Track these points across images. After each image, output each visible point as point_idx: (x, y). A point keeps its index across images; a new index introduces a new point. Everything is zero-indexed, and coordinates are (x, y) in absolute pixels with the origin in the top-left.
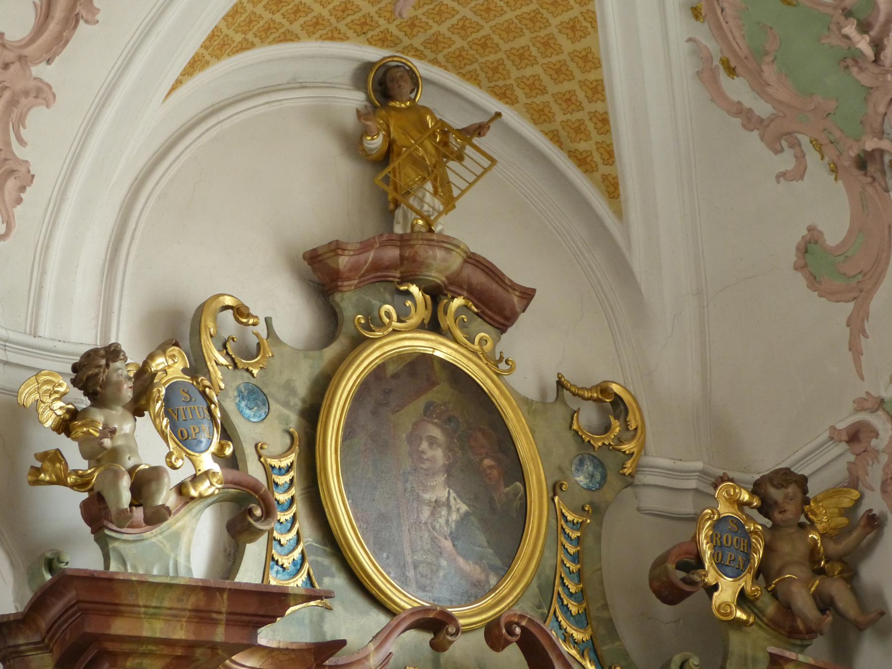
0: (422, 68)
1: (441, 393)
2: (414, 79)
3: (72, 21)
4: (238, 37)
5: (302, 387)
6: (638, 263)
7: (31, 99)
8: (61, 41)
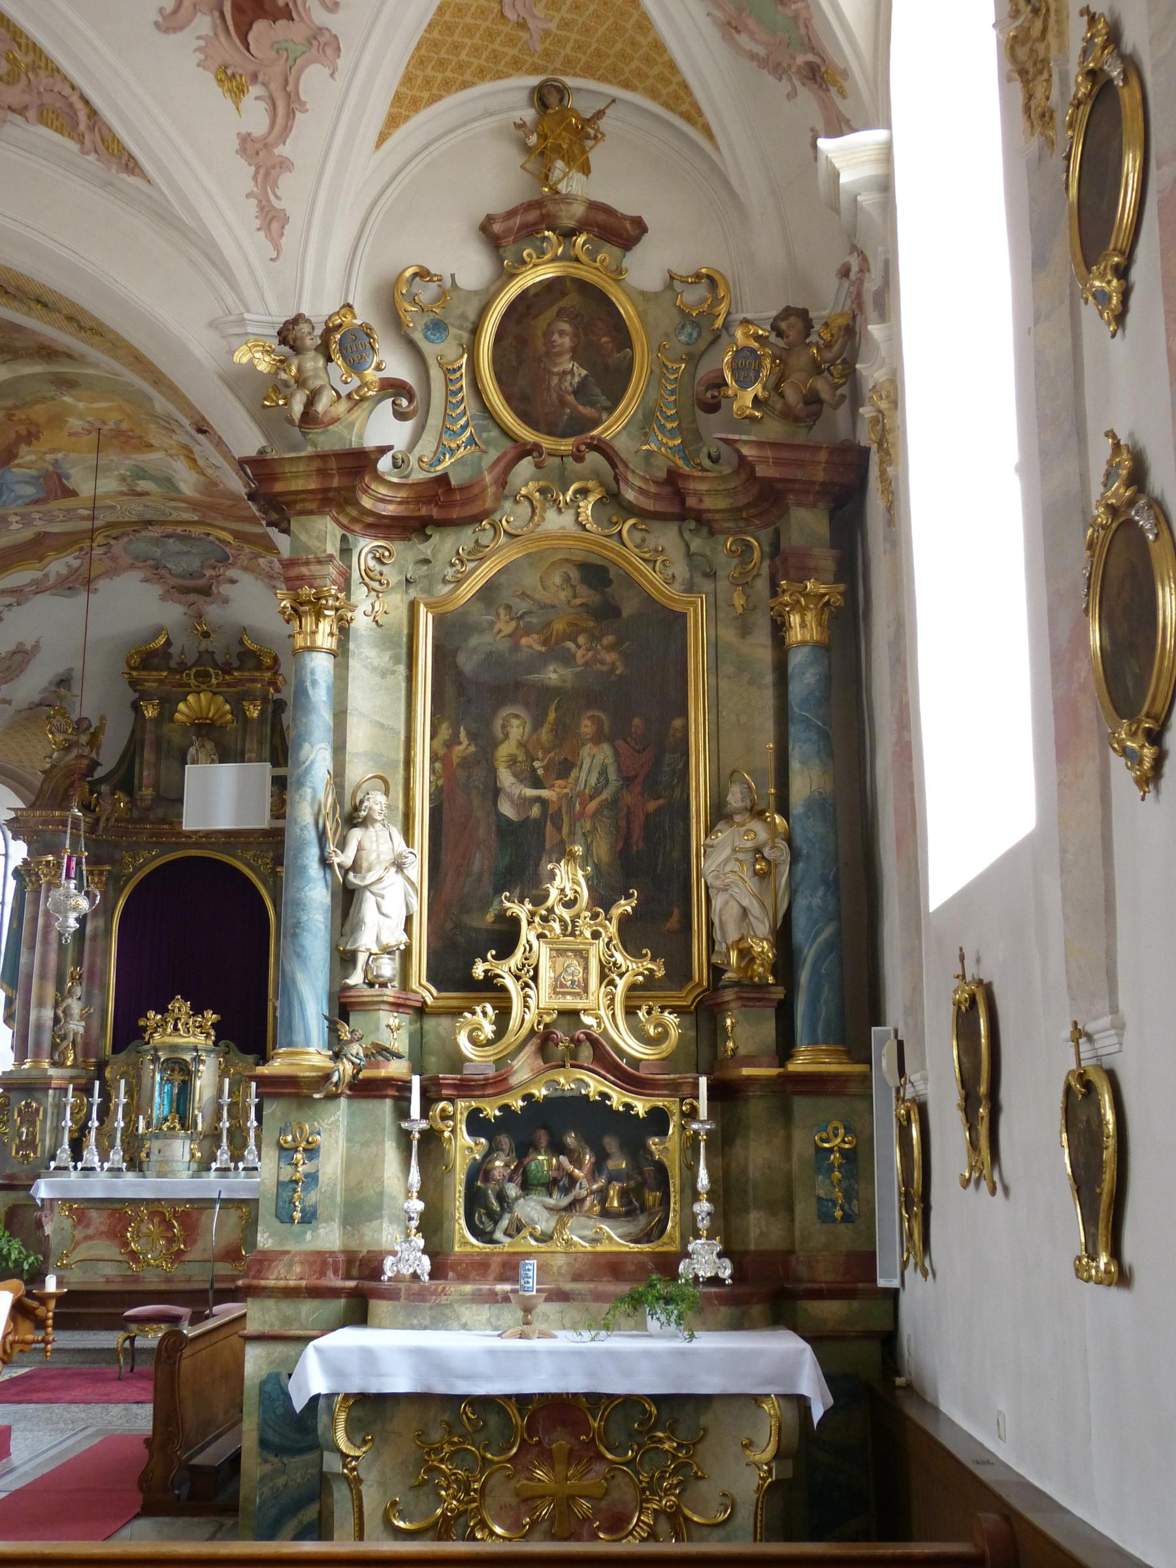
0: (569, 81)
1: (572, 300)
2: (562, 92)
3: (290, 114)
4: (426, 95)
5: (472, 315)
6: (735, 183)
7: (278, 169)
8: (287, 129)
